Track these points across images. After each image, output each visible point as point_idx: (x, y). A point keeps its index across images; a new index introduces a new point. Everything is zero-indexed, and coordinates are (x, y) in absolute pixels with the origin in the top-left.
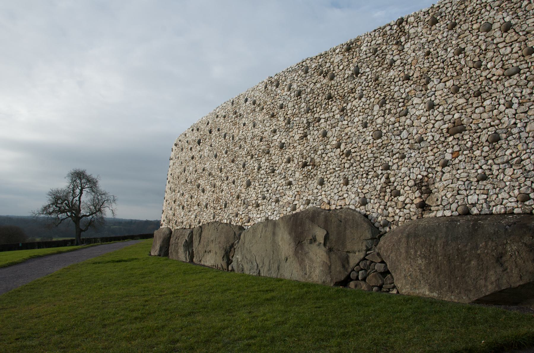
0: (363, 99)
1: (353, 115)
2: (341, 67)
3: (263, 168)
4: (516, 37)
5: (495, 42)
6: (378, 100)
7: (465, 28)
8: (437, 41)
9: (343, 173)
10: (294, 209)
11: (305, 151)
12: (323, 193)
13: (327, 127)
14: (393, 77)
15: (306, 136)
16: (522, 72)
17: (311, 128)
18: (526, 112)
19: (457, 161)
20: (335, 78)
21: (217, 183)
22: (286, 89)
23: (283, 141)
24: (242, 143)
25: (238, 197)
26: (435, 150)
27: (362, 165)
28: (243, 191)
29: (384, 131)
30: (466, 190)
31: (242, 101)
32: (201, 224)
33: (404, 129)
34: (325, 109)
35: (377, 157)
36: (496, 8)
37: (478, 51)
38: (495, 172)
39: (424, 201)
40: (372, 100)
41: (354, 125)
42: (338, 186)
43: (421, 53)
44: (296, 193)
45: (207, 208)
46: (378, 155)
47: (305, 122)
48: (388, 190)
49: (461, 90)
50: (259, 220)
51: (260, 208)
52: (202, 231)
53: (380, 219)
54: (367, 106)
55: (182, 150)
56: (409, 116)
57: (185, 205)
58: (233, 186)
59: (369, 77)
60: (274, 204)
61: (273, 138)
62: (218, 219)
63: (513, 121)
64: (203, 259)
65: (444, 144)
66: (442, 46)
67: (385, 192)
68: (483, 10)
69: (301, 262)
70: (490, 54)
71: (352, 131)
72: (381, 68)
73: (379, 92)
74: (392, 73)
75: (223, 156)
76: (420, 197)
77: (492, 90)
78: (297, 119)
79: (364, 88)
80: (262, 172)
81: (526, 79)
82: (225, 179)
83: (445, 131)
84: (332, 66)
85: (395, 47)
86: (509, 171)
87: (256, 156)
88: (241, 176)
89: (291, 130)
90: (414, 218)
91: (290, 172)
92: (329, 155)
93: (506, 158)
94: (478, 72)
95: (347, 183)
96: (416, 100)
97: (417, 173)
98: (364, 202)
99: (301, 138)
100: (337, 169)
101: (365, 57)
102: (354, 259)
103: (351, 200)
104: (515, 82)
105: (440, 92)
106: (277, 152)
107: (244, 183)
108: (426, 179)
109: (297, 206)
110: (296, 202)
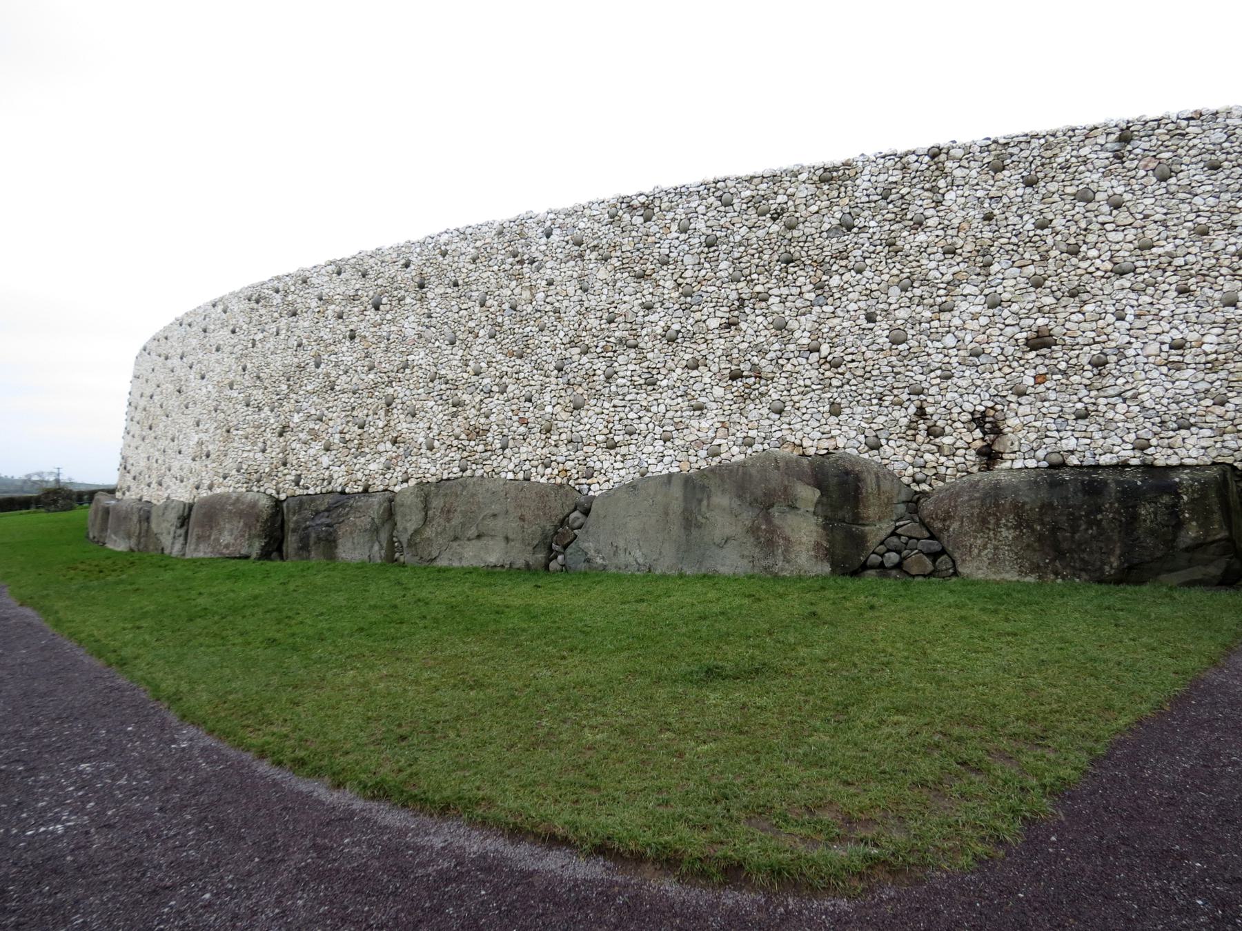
1: (844, 299)
2: (814, 208)
3: (621, 374)
4: (1131, 220)
5: (1101, 219)
6: (897, 280)
8: (1005, 200)
9: (829, 395)
11: (736, 351)
12: (785, 426)
13: (787, 312)
14: (925, 245)
16: (1138, 271)
17: (747, 310)
18: (1144, 329)
19: (1041, 388)
20: (801, 226)
21: (466, 397)
22: (674, 227)
24: (548, 320)
26: (1006, 370)
30: (1058, 431)
32: (412, 482)
33: (948, 332)
35: (899, 373)
36: (1102, 170)
37: (1073, 229)
38: (1102, 408)
39: (989, 446)
41: (847, 316)
42: (819, 416)
43: (976, 214)
44: (719, 425)
46: (902, 370)
48: (922, 427)
49: (1048, 283)
54: (874, 287)
56: (956, 313)
59: (875, 237)
60: (661, 442)
61: (646, 319)
62: (479, 473)
63: (1127, 339)
65: (1022, 362)
66: (1014, 208)
70: (1091, 238)
71: (845, 324)
72: (901, 225)
73: (898, 266)
74: (922, 237)
76: (983, 439)
77: (1093, 291)
79: (866, 254)
83: (1021, 342)
84: (790, 203)
87: (599, 350)
89: (695, 308)
90: (975, 469)
91: (698, 387)
92: (794, 361)
93: (1117, 390)
94: (1074, 260)
96: (969, 289)
97: (973, 403)
100: (814, 387)
101: (865, 199)
104: (1128, 285)
105: (1013, 282)
106: (659, 346)
108: (992, 412)
109: (724, 448)
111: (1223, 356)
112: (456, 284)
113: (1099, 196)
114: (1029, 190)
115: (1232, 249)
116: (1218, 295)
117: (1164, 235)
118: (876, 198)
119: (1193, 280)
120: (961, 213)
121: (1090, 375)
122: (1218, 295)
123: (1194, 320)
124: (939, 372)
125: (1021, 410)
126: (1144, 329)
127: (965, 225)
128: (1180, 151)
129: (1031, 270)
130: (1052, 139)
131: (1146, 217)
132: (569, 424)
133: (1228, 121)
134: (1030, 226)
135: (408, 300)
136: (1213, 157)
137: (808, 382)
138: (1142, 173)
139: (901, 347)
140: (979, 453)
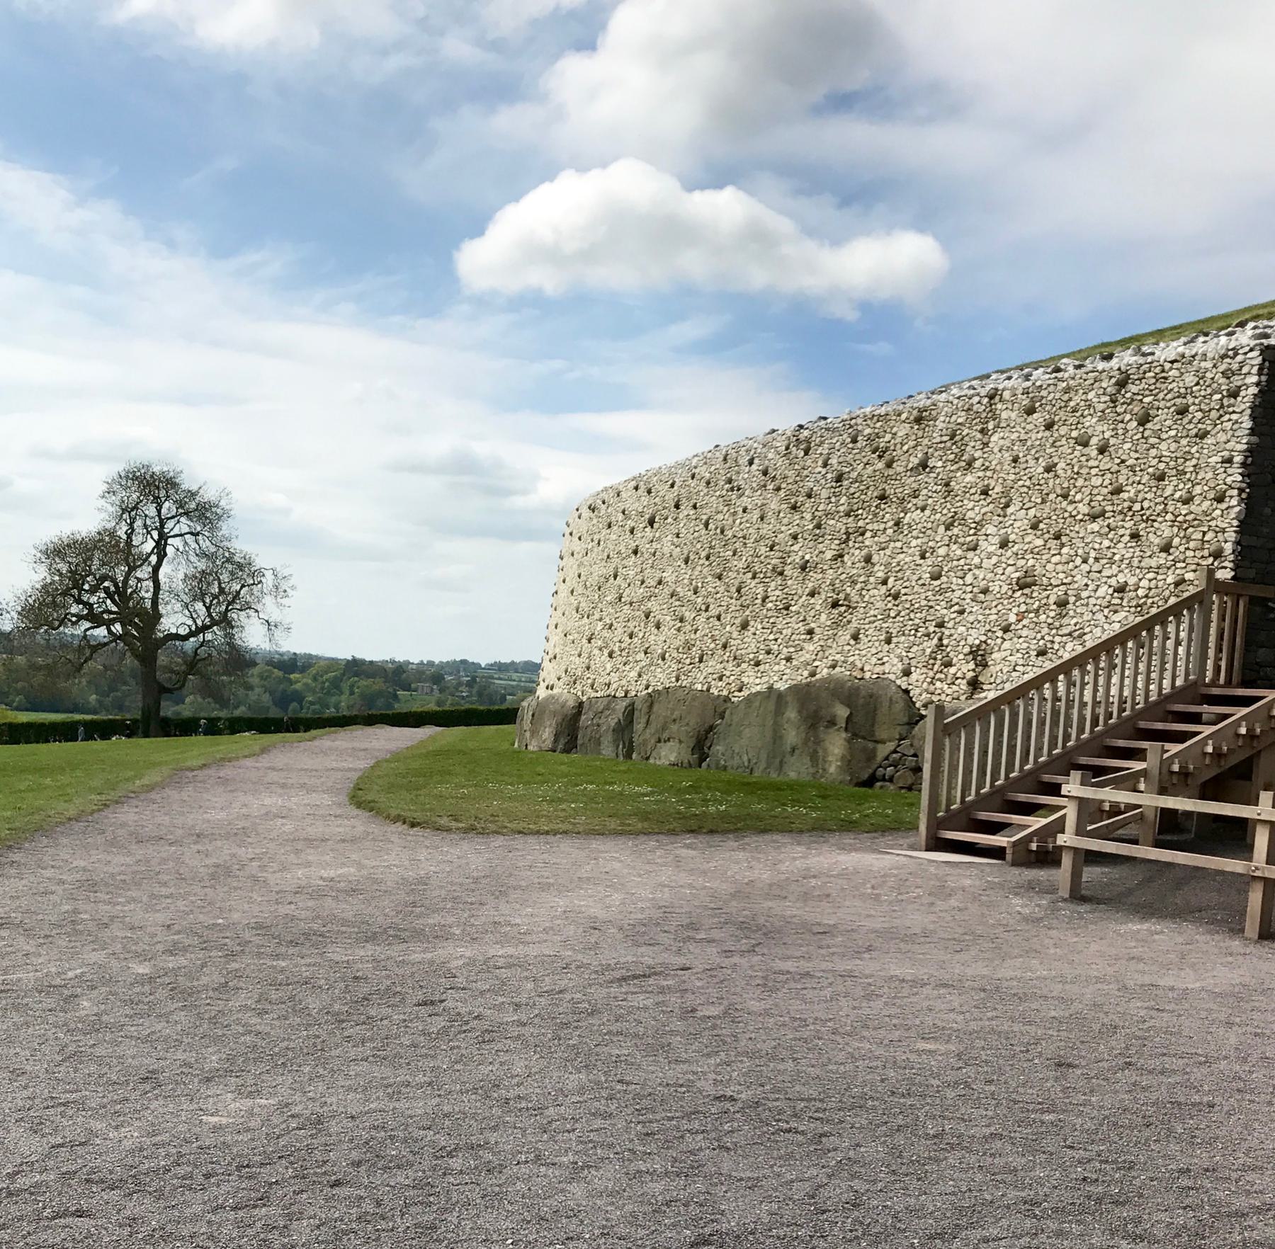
0: (927, 512)
2: (905, 448)
5: (1091, 463)
7: (1062, 433)
8: (1029, 443)
10: (813, 674)
15: (841, 556)
17: (851, 544)
18: (1100, 572)
19: (1020, 626)
21: (687, 614)
22: (820, 463)
23: (807, 557)
25: (725, 646)
27: (912, 616)
28: (735, 635)
29: (946, 569)
31: (744, 461)
32: (650, 690)
34: (875, 515)
37: (1069, 472)
38: (1056, 646)
39: (976, 676)
40: (938, 516)
42: (877, 644)
43: (1008, 456)
45: (664, 659)
47: (843, 531)
48: (939, 657)
49: (1042, 526)
50: (758, 688)
51: (761, 668)
52: (652, 703)
53: (924, 695)
54: (930, 525)
55: (609, 526)
56: (978, 552)
57: (616, 649)
58: (717, 623)
63: (1086, 580)
64: (654, 754)
66: (1033, 452)
67: (935, 659)
68: (1086, 412)
69: (814, 757)
70: (1080, 482)
73: (949, 506)
74: (969, 478)
75: (701, 562)
77: (1072, 535)
78: (832, 522)
80: (770, 605)
81: (1108, 526)
82: (703, 607)
85: (979, 436)
86: (1069, 646)
88: (733, 608)
95: (888, 641)
97: (975, 638)
98: (907, 673)
99: (835, 558)
101: (938, 440)
102: (883, 751)
103: (893, 668)
104: (1096, 529)
107: (738, 621)
109: (819, 670)
110: (816, 663)
111: (1150, 601)
112: (695, 507)
113: (1094, 441)
114: (1047, 433)
115: (1177, 495)
116: (1157, 541)
117: (1130, 481)
118: (945, 438)
119: (1144, 525)
120: (999, 455)
121: (1052, 614)
122: (1157, 541)
123: (1135, 564)
124: (956, 608)
125: (1007, 645)
126: (1100, 572)
127: (998, 468)
128: (1161, 396)
129: (1032, 512)
130: (1071, 382)
131: (1123, 462)
132: (735, 642)
133: (1203, 364)
134: (1041, 470)
135: (670, 520)
136: (1185, 401)
137: (876, 612)
138: (1128, 417)
139: (936, 583)
140: (969, 683)
